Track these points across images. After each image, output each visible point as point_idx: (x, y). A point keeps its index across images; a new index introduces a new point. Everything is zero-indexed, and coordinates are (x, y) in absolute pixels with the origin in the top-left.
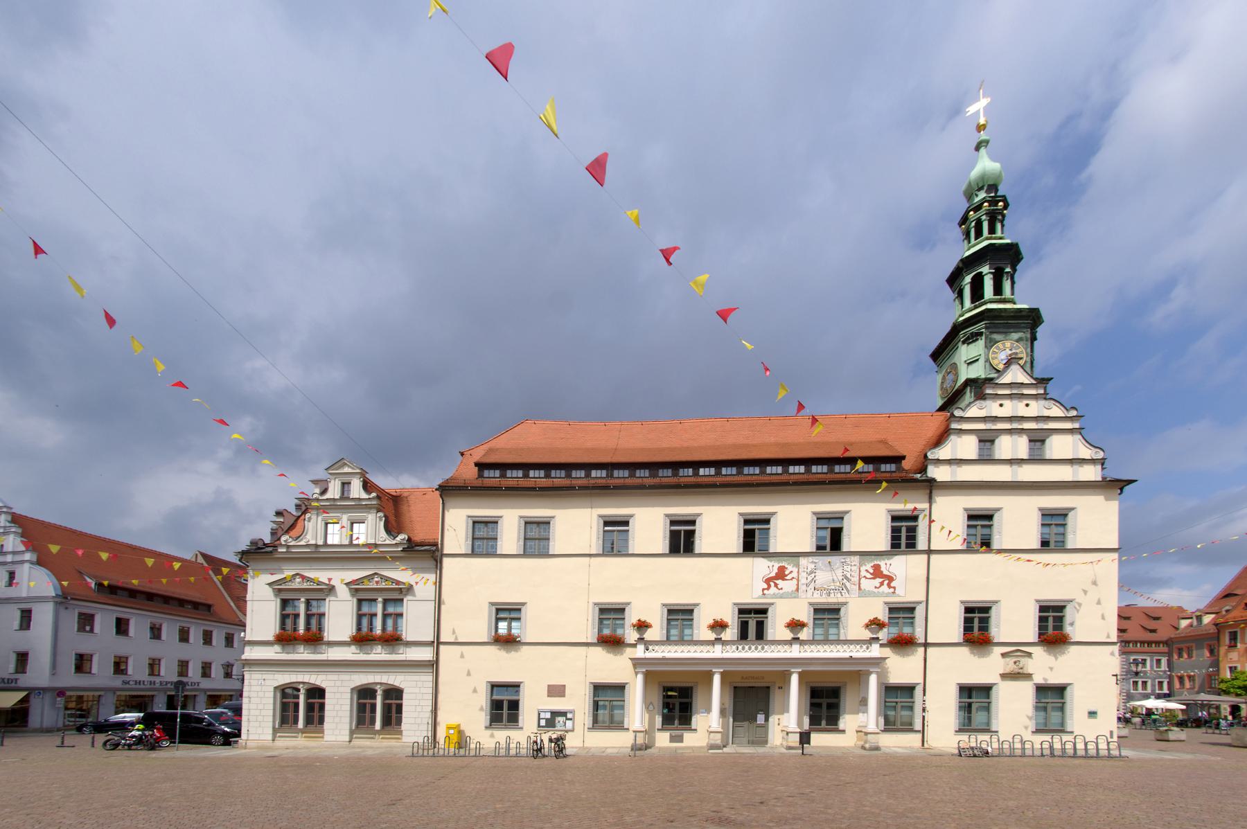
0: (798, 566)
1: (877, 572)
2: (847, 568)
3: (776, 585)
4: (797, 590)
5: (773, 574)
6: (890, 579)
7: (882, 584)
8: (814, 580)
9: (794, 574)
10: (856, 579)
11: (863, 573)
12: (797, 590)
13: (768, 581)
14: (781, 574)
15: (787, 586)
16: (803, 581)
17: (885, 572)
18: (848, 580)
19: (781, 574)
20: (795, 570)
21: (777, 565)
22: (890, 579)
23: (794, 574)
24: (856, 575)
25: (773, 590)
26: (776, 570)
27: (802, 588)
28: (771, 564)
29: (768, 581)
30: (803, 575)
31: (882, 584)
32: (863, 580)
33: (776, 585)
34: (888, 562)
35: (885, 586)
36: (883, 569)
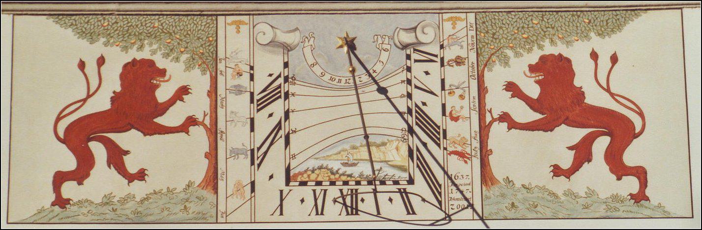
0: (209, 60)
1: (557, 97)
2: (428, 75)
3: (116, 157)
4: (212, 180)
5: (101, 103)
6: (620, 130)
7: (582, 153)
8: (282, 133)
9: (197, 105)
10: (462, 131)
11: (499, 101)
12: (212, 180)
13: (79, 135)
14: (138, 103)
15: (165, 159)
16: (237, 136)
17: (595, 98)
18: (436, 133)
19: (138, 103)
20: (199, 82)
21: (118, 59)
22: (620, 130)
23: (197, 105)
24: (464, 106)
25: (103, 180)
26: (113, 84)
27: (236, 171)
28: (90, 51)
29: (79, 135)
30: (237, 106)
31: (582, 153)
32: (498, 130)
33: (116, 157)
34: (605, 46)
35: (597, 170)
36: (583, 78)
